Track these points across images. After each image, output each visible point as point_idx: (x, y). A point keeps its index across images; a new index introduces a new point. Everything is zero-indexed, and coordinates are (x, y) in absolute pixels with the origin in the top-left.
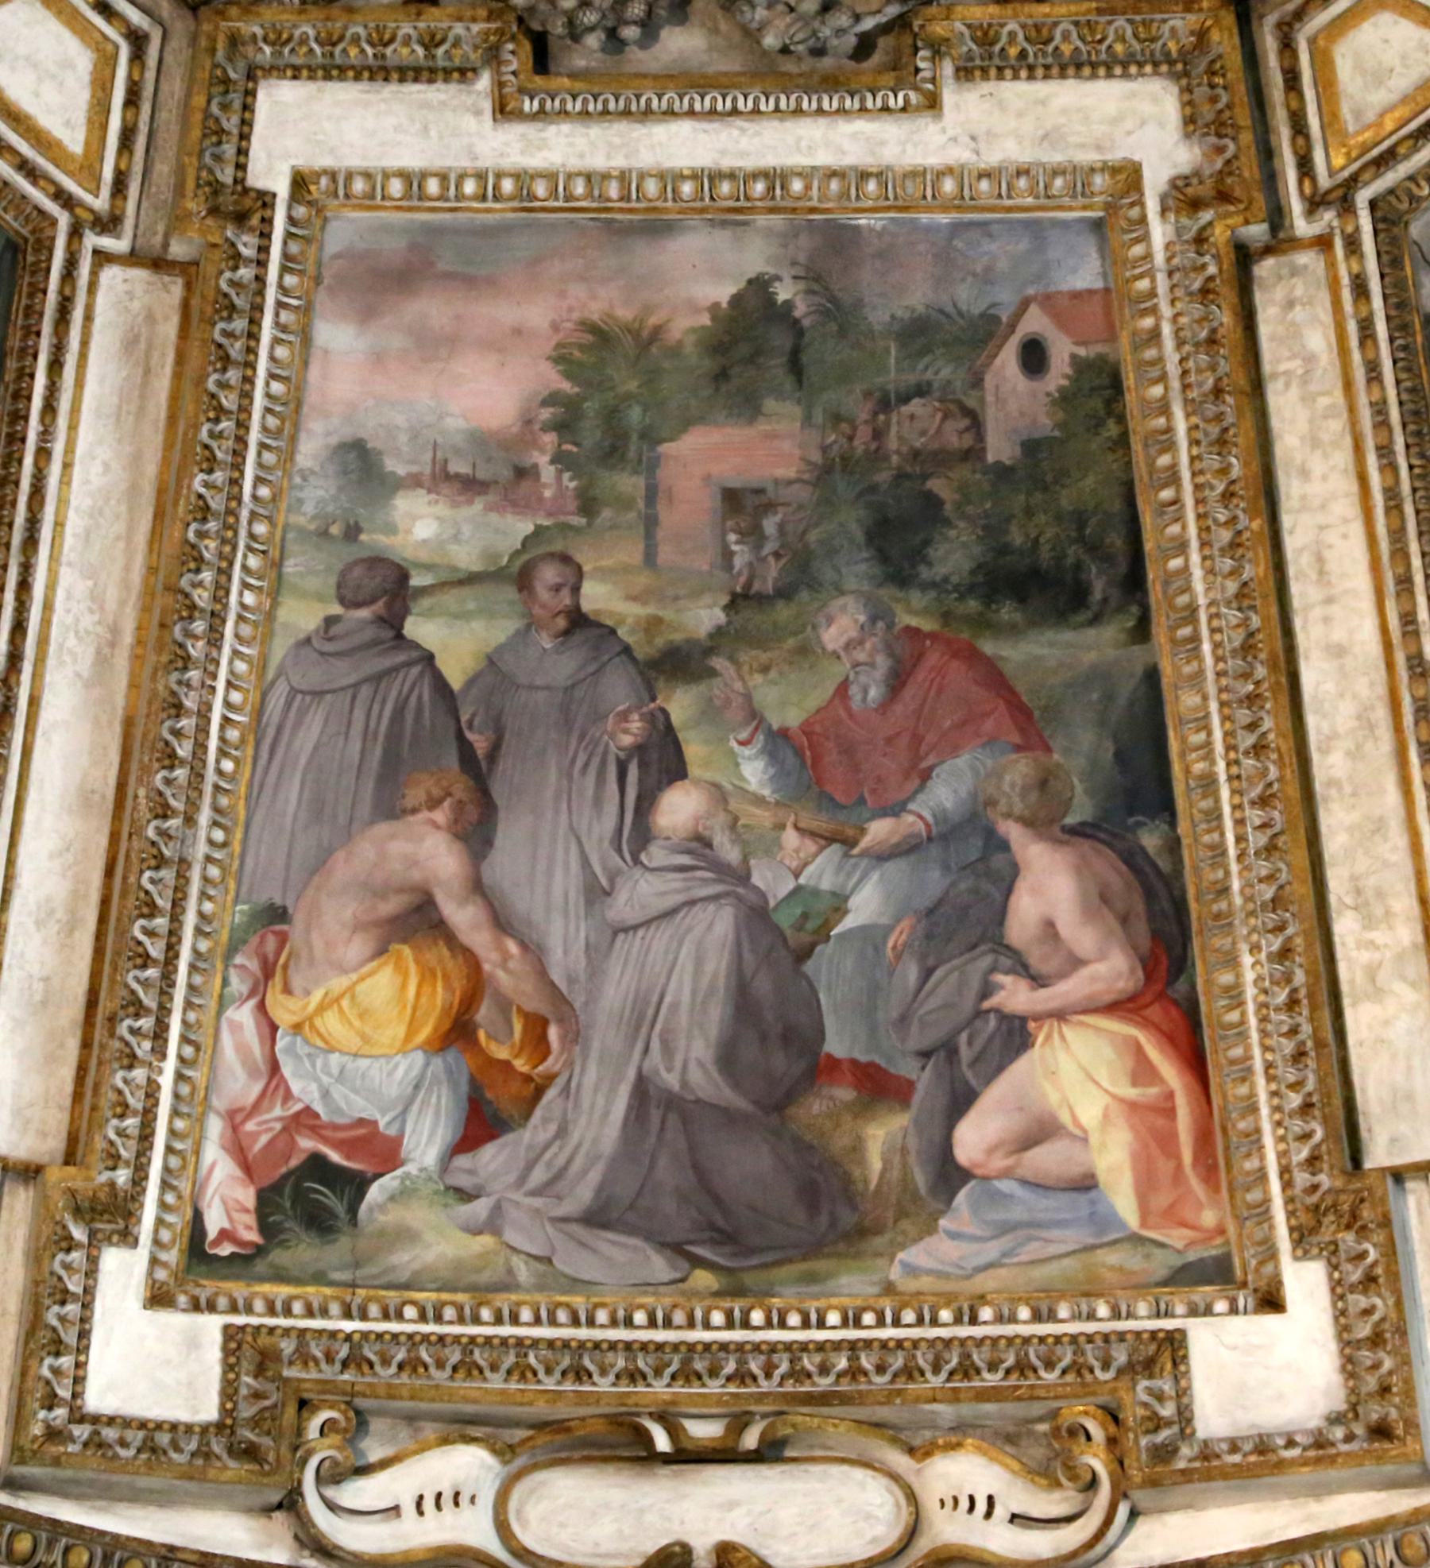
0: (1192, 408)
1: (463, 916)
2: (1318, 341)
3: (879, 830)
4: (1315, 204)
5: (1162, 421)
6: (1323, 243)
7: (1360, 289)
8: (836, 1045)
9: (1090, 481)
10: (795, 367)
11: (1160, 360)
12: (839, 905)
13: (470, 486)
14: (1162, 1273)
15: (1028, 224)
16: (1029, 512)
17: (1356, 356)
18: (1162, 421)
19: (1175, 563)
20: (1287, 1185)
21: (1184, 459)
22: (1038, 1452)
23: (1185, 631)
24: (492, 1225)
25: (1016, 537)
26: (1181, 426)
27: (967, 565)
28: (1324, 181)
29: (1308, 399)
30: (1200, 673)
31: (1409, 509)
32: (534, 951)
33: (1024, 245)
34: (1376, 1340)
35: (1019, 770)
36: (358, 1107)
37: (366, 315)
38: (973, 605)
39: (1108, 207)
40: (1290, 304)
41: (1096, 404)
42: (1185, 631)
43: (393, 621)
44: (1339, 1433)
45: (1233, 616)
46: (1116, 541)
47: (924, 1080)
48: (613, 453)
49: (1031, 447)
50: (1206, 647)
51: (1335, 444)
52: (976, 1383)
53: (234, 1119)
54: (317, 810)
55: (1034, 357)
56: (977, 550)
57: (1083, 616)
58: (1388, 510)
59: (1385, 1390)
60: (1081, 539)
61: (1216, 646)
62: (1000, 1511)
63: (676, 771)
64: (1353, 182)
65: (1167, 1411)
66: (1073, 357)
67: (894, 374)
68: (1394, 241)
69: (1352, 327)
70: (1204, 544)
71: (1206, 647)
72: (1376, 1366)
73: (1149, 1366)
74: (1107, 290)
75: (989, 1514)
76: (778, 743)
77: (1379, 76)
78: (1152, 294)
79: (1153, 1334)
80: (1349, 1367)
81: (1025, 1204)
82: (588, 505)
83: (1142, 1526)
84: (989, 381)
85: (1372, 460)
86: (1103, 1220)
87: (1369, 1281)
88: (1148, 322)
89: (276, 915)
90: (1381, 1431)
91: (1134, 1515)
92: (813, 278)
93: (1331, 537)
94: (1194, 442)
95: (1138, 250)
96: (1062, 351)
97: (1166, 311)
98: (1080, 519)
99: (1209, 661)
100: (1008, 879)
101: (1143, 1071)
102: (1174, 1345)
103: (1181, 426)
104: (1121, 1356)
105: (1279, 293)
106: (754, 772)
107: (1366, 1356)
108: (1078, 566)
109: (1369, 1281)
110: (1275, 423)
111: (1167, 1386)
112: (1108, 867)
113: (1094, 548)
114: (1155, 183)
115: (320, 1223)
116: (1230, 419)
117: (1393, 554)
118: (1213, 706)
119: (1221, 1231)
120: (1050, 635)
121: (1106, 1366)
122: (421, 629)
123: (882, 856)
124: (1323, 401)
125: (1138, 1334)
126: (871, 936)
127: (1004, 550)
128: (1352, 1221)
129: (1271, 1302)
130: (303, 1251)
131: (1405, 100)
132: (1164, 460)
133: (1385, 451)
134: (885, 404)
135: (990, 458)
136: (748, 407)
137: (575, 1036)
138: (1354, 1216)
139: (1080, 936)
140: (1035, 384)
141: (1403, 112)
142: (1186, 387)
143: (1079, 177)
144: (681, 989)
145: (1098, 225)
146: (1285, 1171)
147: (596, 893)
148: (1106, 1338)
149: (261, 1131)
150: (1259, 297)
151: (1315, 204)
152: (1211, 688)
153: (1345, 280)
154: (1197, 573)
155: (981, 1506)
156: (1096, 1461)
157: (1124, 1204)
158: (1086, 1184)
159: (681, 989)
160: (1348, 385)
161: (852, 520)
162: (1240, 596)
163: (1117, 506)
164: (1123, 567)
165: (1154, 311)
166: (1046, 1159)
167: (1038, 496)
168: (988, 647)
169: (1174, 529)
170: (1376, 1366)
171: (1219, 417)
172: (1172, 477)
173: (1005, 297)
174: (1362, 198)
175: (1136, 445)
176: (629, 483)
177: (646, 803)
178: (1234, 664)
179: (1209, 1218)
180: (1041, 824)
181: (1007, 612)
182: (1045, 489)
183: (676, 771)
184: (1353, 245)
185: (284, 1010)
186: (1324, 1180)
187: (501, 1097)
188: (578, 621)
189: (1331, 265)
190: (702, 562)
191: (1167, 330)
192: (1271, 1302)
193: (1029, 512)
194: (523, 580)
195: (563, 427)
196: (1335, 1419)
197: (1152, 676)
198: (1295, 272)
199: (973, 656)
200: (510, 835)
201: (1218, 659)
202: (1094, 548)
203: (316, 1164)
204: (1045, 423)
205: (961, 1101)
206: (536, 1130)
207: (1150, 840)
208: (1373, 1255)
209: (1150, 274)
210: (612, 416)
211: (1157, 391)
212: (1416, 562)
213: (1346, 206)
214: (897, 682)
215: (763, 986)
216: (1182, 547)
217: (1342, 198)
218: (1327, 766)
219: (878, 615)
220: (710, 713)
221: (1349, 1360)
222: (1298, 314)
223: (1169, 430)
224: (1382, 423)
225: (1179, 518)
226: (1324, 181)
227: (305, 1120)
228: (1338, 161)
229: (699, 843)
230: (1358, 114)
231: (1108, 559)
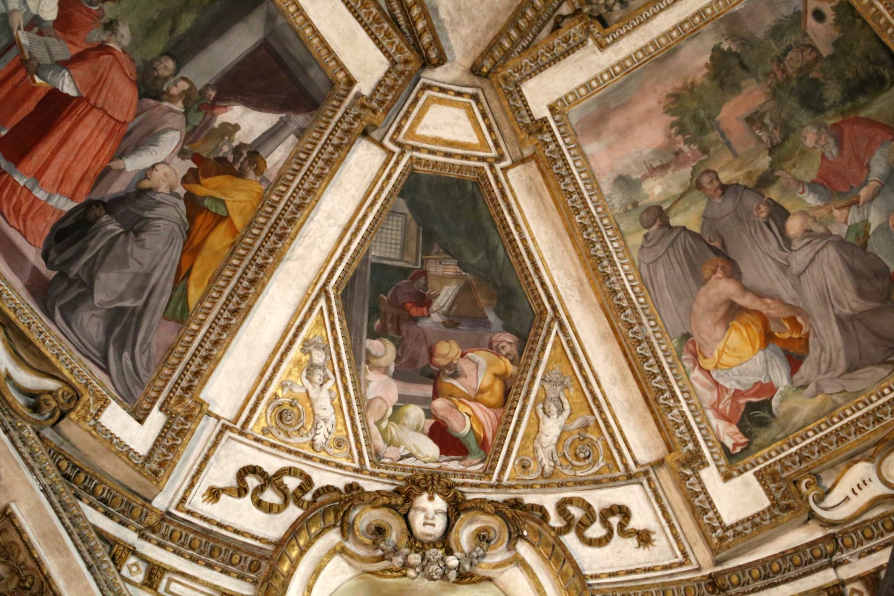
1: (746, 301)
3: (864, 193)
5: (874, 9)
9: (862, 42)
10: (744, 67)
12: (866, 224)
13: (663, 168)
18: (874, 9)
21: (888, 16)
24: (819, 391)
25: (849, 75)
26: (881, 7)
27: (839, 94)
36: (752, 380)
37: (598, 136)
38: (849, 104)
41: (850, 17)
43: (665, 224)
48: (702, 128)
49: (836, 44)
52: (884, 423)
53: (714, 407)
54: (679, 296)
55: (819, 16)
56: (839, 87)
57: (887, 86)
63: (786, 215)
66: (833, 8)
67: (777, 50)
76: (813, 186)
82: (705, 151)
84: (809, 33)
89: (687, 336)
92: (732, 36)
96: (827, 9)
103: (881, 7)
106: (811, 200)
108: (876, 71)
115: (763, 423)
120: (881, 98)
122: (676, 221)
123: (870, 200)
126: (883, 228)
127: (848, 81)
130: (764, 435)
132: (882, 21)
134: (780, 60)
135: (825, 55)
136: (736, 88)
137: (807, 316)
144: (832, 281)
147: (785, 268)
149: (725, 405)
159: (832, 281)
161: (792, 103)
167: (848, 58)
168: (862, 114)
175: (870, 22)
176: (714, 136)
177: (782, 231)
181: (862, 100)
183: (786, 215)
185: (708, 364)
187: (796, 349)
188: (724, 188)
190: (752, 145)
193: (848, 64)
194: (699, 186)
195: (682, 131)
199: (858, 120)
203: (749, 405)
204: (836, 34)
206: (814, 352)
210: (695, 118)
214: (840, 143)
215: (858, 264)
219: (820, 127)
220: (785, 190)
223: (878, 10)
227: (737, 394)
229: (808, 232)
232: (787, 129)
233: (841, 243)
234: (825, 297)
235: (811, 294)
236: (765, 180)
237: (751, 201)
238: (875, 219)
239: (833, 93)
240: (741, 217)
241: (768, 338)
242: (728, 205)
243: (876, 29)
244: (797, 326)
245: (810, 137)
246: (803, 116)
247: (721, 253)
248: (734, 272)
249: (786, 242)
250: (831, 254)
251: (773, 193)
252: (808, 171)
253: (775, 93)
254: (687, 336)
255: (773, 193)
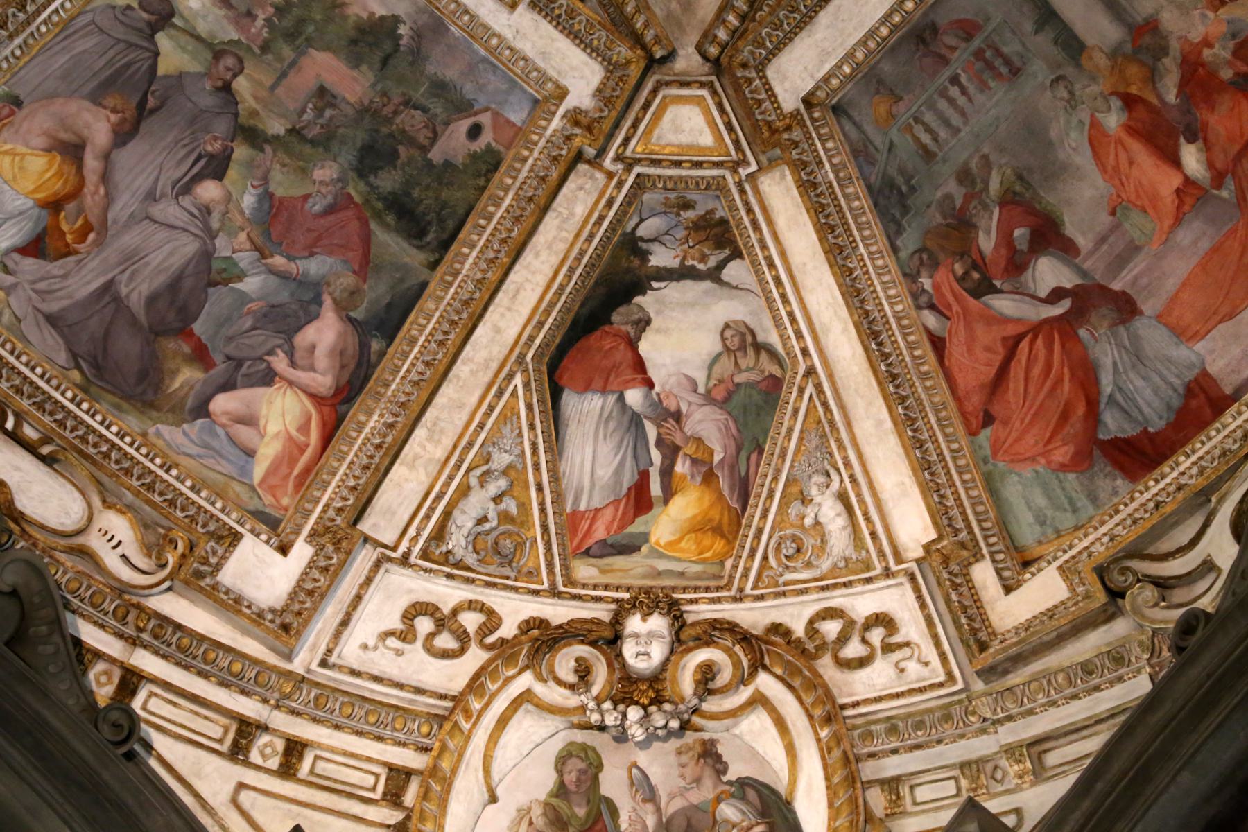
0: (517, 197)
1: (92, 163)
2: (580, 210)
3: (278, 261)
4: (619, 158)
5: (502, 194)
6: (610, 175)
7: (610, 204)
8: (198, 327)
9: (459, 194)
10: (385, 62)
11: (519, 171)
12: (240, 277)
14: (251, 508)
15: (512, 81)
16: (428, 187)
17: (589, 227)
18: (502, 194)
19: (465, 250)
20: (324, 511)
21: (499, 214)
22: (152, 538)
23: (449, 278)
25: (416, 193)
26: (507, 201)
27: (389, 189)
28: (628, 153)
29: (560, 229)
30: (442, 298)
31: (563, 298)
32: (109, 199)
33: (504, 87)
34: (310, 593)
35: (349, 280)
38: (380, 205)
39: (545, 98)
40: (581, 188)
41: (484, 168)
42: (449, 278)
43: (154, 28)
44: (270, 616)
45: (471, 287)
46: (451, 224)
47: (221, 367)
48: (291, 36)
49: (447, 164)
50: (452, 290)
51: (556, 253)
56: (397, 186)
57: (415, 242)
58: (555, 293)
59: (299, 614)
60: (438, 214)
61: (456, 293)
62: (120, 550)
63: (219, 175)
64: (638, 161)
65: (213, 560)
66: (489, 144)
67: (419, 94)
68: (635, 195)
69: (596, 215)
70: (481, 252)
71: (452, 290)
72: (303, 603)
73: (219, 539)
74: (520, 129)
75: (115, 547)
76: (267, 197)
77: (677, 130)
78: (536, 144)
79: (231, 528)
80: (293, 596)
81: (222, 443)
82: (265, 48)
83: (169, 595)
84: (451, 127)
85: (565, 269)
86: (246, 471)
87: (326, 569)
88: (526, 153)
89: (17, 102)
90: (286, 628)
91: (169, 589)
92: (418, 35)
93: (528, 286)
94: (507, 211)
95: (543, 123)
96: (487, 138)
97: (536, 154)
98: (444, 205)
99: (449, 296)
100: (312, 318)
101: (304, 428)
102: (236, 538)
103: (507, 201)
104: (212, 527)
105: (580, 181)
106: (249, 201)
107: (302, 596)
108: (429, 223)
109: (326, 569)
110: (541, 228)
111: (220, 551)
112: (352, 342)
113: (441, 221)
114: (569, 103)
116: (527, 213)
117: (545, 310)
118: (437, 314)
119: (286, 509)
120: (400, 240)
121: (204, 526)
123: (271, 271)
124: (564, 234)
125: (225, 524)
126: (243, 298)
127: (408, 194)
128: (337, 543)
129: (284, 550)
131: (679, 146)
132: (491, 209)
133: (572, 270)
134: (407, 103)
135: (430, 156)
136: (355, 61)
137: (99, 243)
138: (339, 542)
139: (322, 359)
140: (467, 142)
141: (676, 150)
142: (520, 188)
143: (544, 78)
144: (156, 259)
145: (536, 101)
146: (327, 506)
147: (151, 196)
148: (212, 516)
150: (572, 177)
151: (619, 158)
152: (442, 307)
153: (607, 196)
154: (470, 260)
155: (114, 542)
156: (171, 559)
157: (259, 471)
158: (250, 453)
159: (156, 259)
160: (578, 235)
161: (361, 137)
162: (479, 281)
163: (461, 211)
164: (445, 236)
165: (531, 150)
166: (243, 432)
168: (373, 226)
169: (475, 237)
170: (303, 603)
171: (524, 209)
172: (489, 218)
173: (482, 101)
174: (637, 169)
176: (287, 52)
177: (198, 178)
178: (457, 305)
179: (285, 501)
180: (342, 308)
181: (390, 219)
182: (440, 183)
183: (219, 175)
184: (620, 184)
186: (339, 520)
187: (51, 244)
188: (226, 88)
189: (606, 186)
190: (292, 106)
191: (530, 161)
192: (284, 550)
193: (428, 187)
196: (273, 611)
197: (424, 285)
198: (592, 177)
199: (365, 223)
200: (134, 148)
201: (453, 298)
202: (441, 221)
204: (459, 160)
205: (228, 386)
206: (55, 268)
207: (375, 345)
208: (334, 561)
209: (541, 136)
210: (302, 22)
211: (509, 181)
212: (550, 320)
213: (629, 168)
214: (330, 210)
215: (188, 283)
216: (472, 246)
217: (630, 164)
218: (461, 369)
220: (250, 165)
221: (295, 593)
222: (581, 194)
223: (502, 199)
224: (578, 259)
225: (480, 235)
226: (628, 153)
228: (639, 149)
229: (206, 210)
230: (659, 137)
231: (443, 229)
232: (325, 142)
233: (206, 255)
234: (131, 258)
235: (130, 239)
236: (254, 137)
237: (222, 126)
238: (251, 284)
239: (388, 181)
240: (197, 121)
241: (54, 206)
242: (207, 100)
243: (479, 206)
244: (82, 235)
245: (326, 172)
246: (348, 156)
247: (142, 112)
248: (123, 135)
249: (186, 188)
250: (188, 247)
251: (241, 152)
252: (283, 185)
253: (365, 111)
254: (17, 102)
255: (241, 152)
